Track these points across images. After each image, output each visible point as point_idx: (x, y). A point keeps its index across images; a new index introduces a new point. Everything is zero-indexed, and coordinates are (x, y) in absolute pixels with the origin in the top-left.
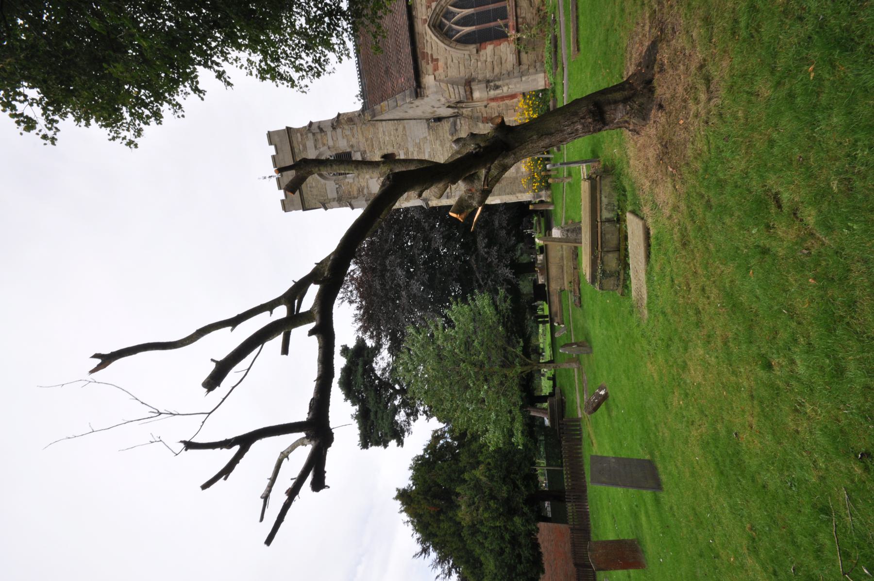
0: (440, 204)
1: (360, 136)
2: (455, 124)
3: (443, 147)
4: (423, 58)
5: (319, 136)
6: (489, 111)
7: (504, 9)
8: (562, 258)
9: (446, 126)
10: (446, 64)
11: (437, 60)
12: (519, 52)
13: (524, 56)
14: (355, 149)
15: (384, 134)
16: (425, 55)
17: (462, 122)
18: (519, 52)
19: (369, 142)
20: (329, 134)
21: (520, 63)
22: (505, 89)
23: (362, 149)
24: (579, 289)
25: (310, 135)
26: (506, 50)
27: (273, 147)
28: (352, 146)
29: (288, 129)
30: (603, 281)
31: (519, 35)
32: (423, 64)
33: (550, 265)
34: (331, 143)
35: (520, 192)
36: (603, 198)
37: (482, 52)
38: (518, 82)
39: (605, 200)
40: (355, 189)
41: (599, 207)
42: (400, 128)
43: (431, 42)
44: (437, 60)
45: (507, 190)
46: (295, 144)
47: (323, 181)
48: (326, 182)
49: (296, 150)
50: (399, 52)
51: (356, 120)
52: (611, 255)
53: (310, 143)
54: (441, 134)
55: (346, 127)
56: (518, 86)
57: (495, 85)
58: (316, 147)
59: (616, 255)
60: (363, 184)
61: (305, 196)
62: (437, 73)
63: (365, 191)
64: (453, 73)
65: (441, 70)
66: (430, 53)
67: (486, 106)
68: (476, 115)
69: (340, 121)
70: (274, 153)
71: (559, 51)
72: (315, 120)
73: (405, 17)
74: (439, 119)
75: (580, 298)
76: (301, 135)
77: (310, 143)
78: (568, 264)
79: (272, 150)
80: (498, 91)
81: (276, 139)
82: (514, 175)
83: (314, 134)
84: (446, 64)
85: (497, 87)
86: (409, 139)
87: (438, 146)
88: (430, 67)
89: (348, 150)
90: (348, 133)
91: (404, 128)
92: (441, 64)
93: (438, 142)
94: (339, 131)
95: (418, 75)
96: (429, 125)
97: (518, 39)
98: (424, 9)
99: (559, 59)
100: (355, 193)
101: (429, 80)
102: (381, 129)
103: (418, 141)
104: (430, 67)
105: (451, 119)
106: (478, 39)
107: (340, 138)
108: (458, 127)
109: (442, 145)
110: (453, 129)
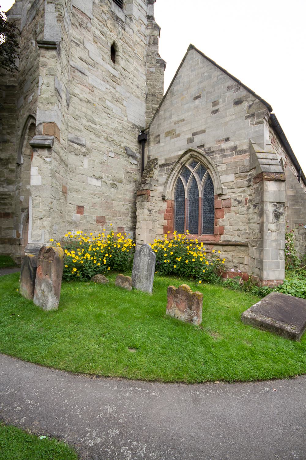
1: (138, 40)
2: (135, 158)
9: (134, 146)
15: (136, 69)
17: (134, 167)
19: (131, 43)
22: (273, 227)
38: (279, 245)
45: (55, 201)
51: (153, 49)
54: (127, 136)
55: (148, 32)
56: (274, 244)
57: (281, 214)
68: (153, 183)
80: (271, 217)
86: (128, 95)
91: (138, 97)
93: (120, 128)
94: (145, 20)
96: (137, 127)
102: (140, 69)
103: (125, 103)
105: (139, 156)
109: (115, 130)
110: (130, 153)
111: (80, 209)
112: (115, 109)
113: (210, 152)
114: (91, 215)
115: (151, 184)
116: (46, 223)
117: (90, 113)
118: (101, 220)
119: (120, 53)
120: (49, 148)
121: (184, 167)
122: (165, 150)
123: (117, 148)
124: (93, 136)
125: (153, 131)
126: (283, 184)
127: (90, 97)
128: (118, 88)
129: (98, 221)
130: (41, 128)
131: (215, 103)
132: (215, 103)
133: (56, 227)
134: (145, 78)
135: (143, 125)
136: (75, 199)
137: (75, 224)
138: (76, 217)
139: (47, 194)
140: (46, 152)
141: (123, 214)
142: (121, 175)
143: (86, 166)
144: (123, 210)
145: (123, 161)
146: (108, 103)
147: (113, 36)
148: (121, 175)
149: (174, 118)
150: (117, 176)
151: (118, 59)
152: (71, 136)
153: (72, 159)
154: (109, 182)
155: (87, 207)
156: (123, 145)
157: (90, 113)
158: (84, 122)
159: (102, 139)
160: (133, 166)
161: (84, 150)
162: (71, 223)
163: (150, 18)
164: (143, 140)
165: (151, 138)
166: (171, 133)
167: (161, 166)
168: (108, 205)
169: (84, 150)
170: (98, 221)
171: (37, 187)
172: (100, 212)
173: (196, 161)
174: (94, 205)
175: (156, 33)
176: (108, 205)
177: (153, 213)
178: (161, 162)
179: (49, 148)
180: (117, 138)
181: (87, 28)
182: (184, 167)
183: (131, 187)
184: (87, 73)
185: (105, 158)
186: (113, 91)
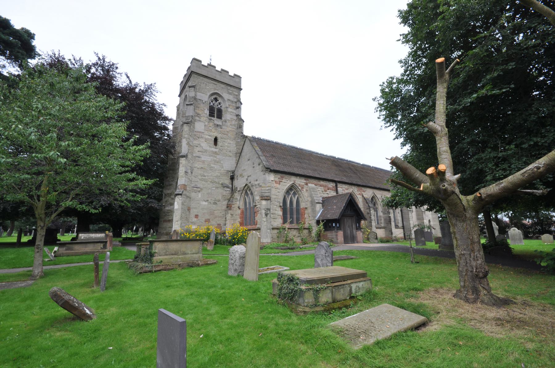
0: (181, 166)
1: (230, 129)
2: (228, 187)
3: (215, 177)
4: (281, 177)
5: (234, 105)
6: (235, 209)
7: (293, 223)
8: (184, 254)
9: (227, 182)
10: (277, 188)
11: (279, 184)
12: (277, 229)
13: (276, 231)
14: (224, 123)
15: (229, 143)
16: (282, 177)
18: (277, 229)
20: (235, 111)
21: (273, 229)
22: (265, 219)
23: (223, 127)
24: (160, 270)
25: (236, 100)
26: (278, 222)
27: (233, 75)
28: (226, 122)
29: (241, 89)
30: (311, 292)
31: (287, 229)
32: (279, 176)
33: (180, 243)
34: (229, 110)
35: (181, 224)
36: (362, 283)
37: (279, 209)
39: (360, 285)
40: (200, 112)
41: (358, 280)
42: (231, 155)
43: (288, 182)
44: (279, 184)
46: (232, 89)
47: (209, 94)
48: (208, 96)
49: (229, 88)
50: (284, 165)
51: (239, 130)
52: (330, 295)
53: (231, 98)
54: (223, 178)
55: (237, 123)
58: (229, 100)
59: (330, 300)
60: (202, 119)
61: (202, 78)
62: (274, 182)
63: (197, 118)
64: (274, 191)
65: (275, 185)
66: (283, 181)
67: (239, 207)
68: (234, 201)
69: (240, 121)
70: (230, 74)
71: (290, 251)
72: (242, 107)
73: (297, 173)
74: (232, 178)
75: (150, 272)
76: (237, 95)
77: (231, 98)
78: (179, 259)
79: (231, 74)
80: (264, 215)
81: (237, 80)
82: (190, 220)
83: (236, 102)
84: (277, 188)
85: (266, 215)
87: (217, 174)
88: (277, 179)
89: (223, 118)
90: (233, 122)
92: (278, 185)
93: (219, 175)
94: (235, 118)
95: (276, 172)
97: (285, 229)
98: (299, 183)
99: (288, 251)
100: (197, 111)
101: (272, 177)
103: (222, 162)
104: (277, 179)
105: (231, 186)
106: (284, 208)
107: (231, 116)
108: (226, 189)
109: (217, 176)
111: (197, 216)
112: (216, 167)
113: (252, 186)
114: (202, 219)
115: (232, 201)
116: (179, 223)
117: (202, 172)
118: (208, 221)
119: (219, 140)
120: (181, 194)
121: (246, 191)
122: (240, 183)
123: (217, 185)
124: (204, 183)
125: (236, 173)
126: (269, 201)
127: (202, 166)
128: (218, 157)
129: (206, 221)
130: (179, 187)
131: (253, 164)
132: (253, 164)
133: (183, 224)
134: (235, 145)
135: (233, 169)
136: (194, 212)
137: (194, 223)
138: (194, 220)
139: (180, 212)
140: (180, 196)
141: (220, 217)
142: (220, 197)
143: (200, 196)
144: (221, 215)
145: (221, 190)
146: (212, 165)
147: (215, 134)
148: (220, 197)
149: (242, 168)
150: (217, 198)
151: (218, 143)
152: (192, 185)
153: (193, 195)
154: (212, 202)
155: (200, 215)
156: (220, 183)
157: (202, 172)
158: (200, 177)
159: (209, 182)
160: (227, 192)
161: (199, 189)
162: (192, 222)
163: (238, 116)
164: (232, 178)
165: (235, 177)
166: (241, 175)
167: (239, 191)
168: (212, 213)
169: (199, 189)
170: (206, 221)
171: (177, 209)
172: (207, 217)
173: (247, 190)
174: (204, 214)
175: (240, 122)
176: (212, 213)
177: (234, 215)
178: (238, 189)
179: (181, 194)
180: (217, 180)
181: (202, 137)
182: (246, 191)
183: (225, 203)
184: (202, 156)
185: (210, 191)
186: (215, 159)
